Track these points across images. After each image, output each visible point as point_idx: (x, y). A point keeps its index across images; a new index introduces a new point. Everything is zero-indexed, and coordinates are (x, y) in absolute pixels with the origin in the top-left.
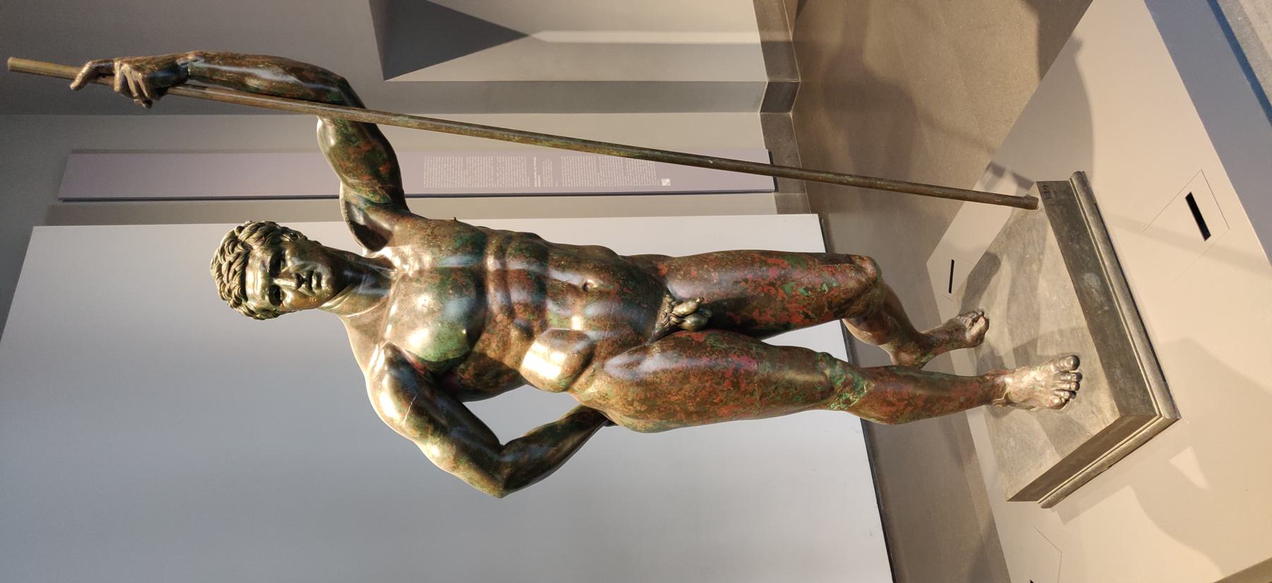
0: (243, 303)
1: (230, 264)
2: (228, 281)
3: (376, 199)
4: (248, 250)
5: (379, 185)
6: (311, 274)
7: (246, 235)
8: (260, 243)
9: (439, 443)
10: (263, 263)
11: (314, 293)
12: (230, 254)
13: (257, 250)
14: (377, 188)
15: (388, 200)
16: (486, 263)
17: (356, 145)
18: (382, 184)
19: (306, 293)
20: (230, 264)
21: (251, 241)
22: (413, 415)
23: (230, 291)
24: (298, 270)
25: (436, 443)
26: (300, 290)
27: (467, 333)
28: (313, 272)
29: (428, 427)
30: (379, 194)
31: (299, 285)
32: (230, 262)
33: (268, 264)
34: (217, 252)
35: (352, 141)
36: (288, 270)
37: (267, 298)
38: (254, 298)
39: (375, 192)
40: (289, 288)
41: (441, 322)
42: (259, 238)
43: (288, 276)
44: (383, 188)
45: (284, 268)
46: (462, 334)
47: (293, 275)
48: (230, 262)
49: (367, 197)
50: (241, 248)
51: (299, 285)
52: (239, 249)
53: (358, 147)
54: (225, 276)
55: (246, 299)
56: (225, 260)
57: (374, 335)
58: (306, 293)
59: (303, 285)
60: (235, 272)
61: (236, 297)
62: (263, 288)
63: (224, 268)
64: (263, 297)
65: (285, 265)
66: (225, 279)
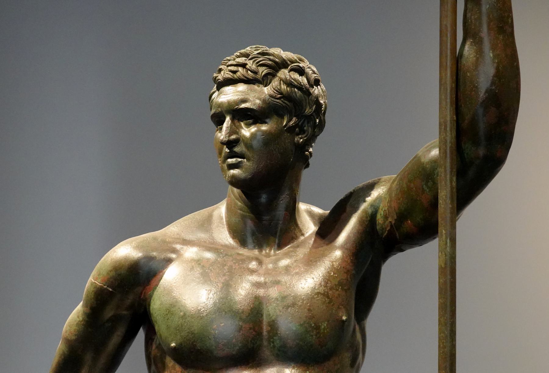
1: (244, 66)
3: (380, 218)
4: (265, 81)
5: (393, 222)
7: (283, 77)
8: (272, 93)
9: (78, 320)
10: (244, 101)
13: (267, 90)
14: (390, 220)
15: (382, 234)
16: (273, 366)
18: (394, 224)
21: (275, 83)
22: (95, 289)
24: (243, 140)
25: (78, 317)
27: (175, 348)
29: (87, 307)
30: (385, 222)
32: (246, 64)
33: (243, 106)
34: (264, 48)
35: (427, 182)
36: (242, 128)
39: (386, 217)
41: (185, 314)
43: (233, 130)
44: (391, 226)
46: (172, 341)
47: (233, 137)
48: (246, 64)
49: (381, 208)
50: (263, 74)
53: (423, 191)
58: (223, 154)
60: (234, 72)
66: (230, 63)
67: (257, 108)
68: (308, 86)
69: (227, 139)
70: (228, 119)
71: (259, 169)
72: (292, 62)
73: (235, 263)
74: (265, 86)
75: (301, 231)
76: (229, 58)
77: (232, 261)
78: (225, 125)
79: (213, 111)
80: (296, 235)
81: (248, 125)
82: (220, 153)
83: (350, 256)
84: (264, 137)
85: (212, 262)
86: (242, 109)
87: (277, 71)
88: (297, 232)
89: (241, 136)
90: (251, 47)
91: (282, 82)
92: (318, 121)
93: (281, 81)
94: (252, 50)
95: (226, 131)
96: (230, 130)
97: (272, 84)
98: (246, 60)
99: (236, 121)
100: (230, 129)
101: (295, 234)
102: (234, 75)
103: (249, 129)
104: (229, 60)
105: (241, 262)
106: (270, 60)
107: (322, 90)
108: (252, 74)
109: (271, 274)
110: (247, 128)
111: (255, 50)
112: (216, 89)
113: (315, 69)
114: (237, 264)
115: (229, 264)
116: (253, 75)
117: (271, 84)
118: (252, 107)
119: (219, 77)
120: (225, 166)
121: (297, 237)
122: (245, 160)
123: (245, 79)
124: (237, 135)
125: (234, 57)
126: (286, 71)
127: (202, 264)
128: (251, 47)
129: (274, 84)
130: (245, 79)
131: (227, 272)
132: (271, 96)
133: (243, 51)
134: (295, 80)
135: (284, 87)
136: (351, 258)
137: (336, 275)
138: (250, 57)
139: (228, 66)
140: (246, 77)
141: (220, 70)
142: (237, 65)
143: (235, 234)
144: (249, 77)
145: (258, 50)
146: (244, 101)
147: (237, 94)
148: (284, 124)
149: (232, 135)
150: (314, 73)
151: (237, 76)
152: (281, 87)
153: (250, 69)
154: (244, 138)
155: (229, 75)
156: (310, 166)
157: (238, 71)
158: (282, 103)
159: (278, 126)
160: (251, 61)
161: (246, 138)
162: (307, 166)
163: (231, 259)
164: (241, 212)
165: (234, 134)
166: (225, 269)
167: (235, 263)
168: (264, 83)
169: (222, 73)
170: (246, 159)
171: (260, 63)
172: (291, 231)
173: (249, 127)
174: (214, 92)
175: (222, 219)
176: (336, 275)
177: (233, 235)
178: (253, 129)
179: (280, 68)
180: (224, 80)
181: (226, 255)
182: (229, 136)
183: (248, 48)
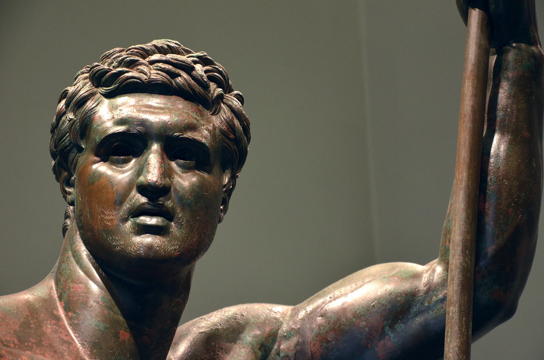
0: (102, 90)
2: (152, 63)
6: (168, 215)
10: (192, 127)
11: (125, 220)
12: (206, 72)
17: (387, 328)
19: (126, 206)
20: (189, 69)
23: (132, 64)
26: (134, 192)
31: (143, 189)
33: (189, 135)
37: (121, 129)
38: (113, 108)
40: (139, 172)
42: (230, 125)
43: (166, 173)
45: (179, 165)
48: (193, 69)
51: (143, 189)
52: (216, 90)
54: (164, 58)
55: (109, 95)
56: (195, 62)
57: (20, 341)
59: (144, 200)
60: (174, 75)
61: (122, 73)
62: (143, 123)
64: (121, 122)
65: (186, 169)
86: (187, 139)
123: (191, 92)
130: (191, 92)
132: (221, 131)
143: (95, 351)
146: (192, 127)
154: (178, 188)
161: (184, 189)
177: (91, 351)
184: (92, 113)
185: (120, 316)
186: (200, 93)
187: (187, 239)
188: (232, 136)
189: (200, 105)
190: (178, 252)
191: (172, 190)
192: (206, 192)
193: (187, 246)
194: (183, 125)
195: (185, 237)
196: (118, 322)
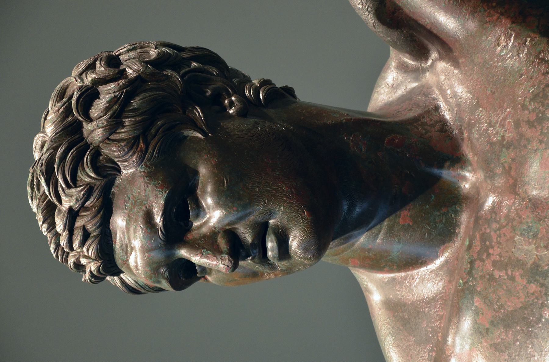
28: (266, 224)
33: (158, 220)
47: (222, 242)
50: (92, 175)
60: (86, 236)
63: (60, 226)
66: (63, 242)
67: (165, 192)
68: (122, 82)
69: (227, 256)
70: (183, 253)
71: (292, 193)
72: (68, 111)
73: (489, 255)
74: (120, 171)
75: (428, 112)
76: (52, 247)
77: (483, 261)
78: (196, 259)
79: (165, 285)
80: (436, 122)
81: (199, 209)
82: (255, 275)
83: (488, 9)
84: (227, 180)
85: (485, 303)
87: (87, 146)
88: (431, 120)
89: (222, 229)
90: (30, 200)
91: (112, 137)
92: (194, 64)
93: (112, 137)
94: (38, 195)
95: (208, 258)
96: (207, 250)
97: (117, 157)
98: (60, 211)
99: (190, 236)
100: (205, 250)
101: (433, 126)
102: (91, 235)
103: (207, 211)
104: (58, 245)
105: (487, 243)
106: (63, 159)
107: (129, 51)
108: (92, 199)
109: (516, 180)
110: (206, 214)
111: (38, 189)
112: (116, 278)
113: (82, 66)
114: (491, 251)
115: (489, 267)
116: (94, 196)
117: (116, 160)
118: (162, 202)
119: (93, 270)
120: (281, 265)
121: (440, 121)
122: (271, 221)
123: (101, 213)
124: (219, 236)
125: (49, 236)
126: (87, 127)
127: (488, 326)
128: (30, 200)
129: (116, 154)
130: (101, 213)
131: (507, 274)
132: (141, 160)
133: (40, 217)
134: (107, 110)
135: (123, 133)
136: (494, 4)
137: (528, 40)
138: (56, 202)
139: (72, 249)
140: (98, 212)
141: (79, 266)
142: (70, 228)
144: (98, 204)
145: (39, 182)
147: (132, 231)
148: (200, 135)
149: (218, 246)
150: (91, 67)
151: (94, 231)
152: (122, 140)
153: (82, 201)
155: (90, 249)
156: (289, 86)
157: (84, 227)
158: (156, 139)
159: (205, 149)
160: (64, 198)
162: (289, 91)
163: (478, 263)
164: (381, 236)
165: (216, 241)
166: (500, 276)
167: (489, 255)
168: (111, 174)
169: (83, 261)
170: (270, 219)
171: (69, 181)
172: (426, 133)
173: (204, 210)
174: (123, 282)
175: (393, 280)
176: (528, 40)
178: (209, 201)
179: (82, 138)
180: (100, 258)
181: (470, 273)
182: (221, 252)
183: (34, 206)
184: (147, 287)
185: (382, 225)
186: (99, 197)
187: (285, 202)
188: (142, 145)
189: (113, 190)
190: (304, 213)
191: (230, 227)
192: (224, 183)
193: (295, 200)
194: (149, 231)
195: (284, 207)
196: (391, 228)
